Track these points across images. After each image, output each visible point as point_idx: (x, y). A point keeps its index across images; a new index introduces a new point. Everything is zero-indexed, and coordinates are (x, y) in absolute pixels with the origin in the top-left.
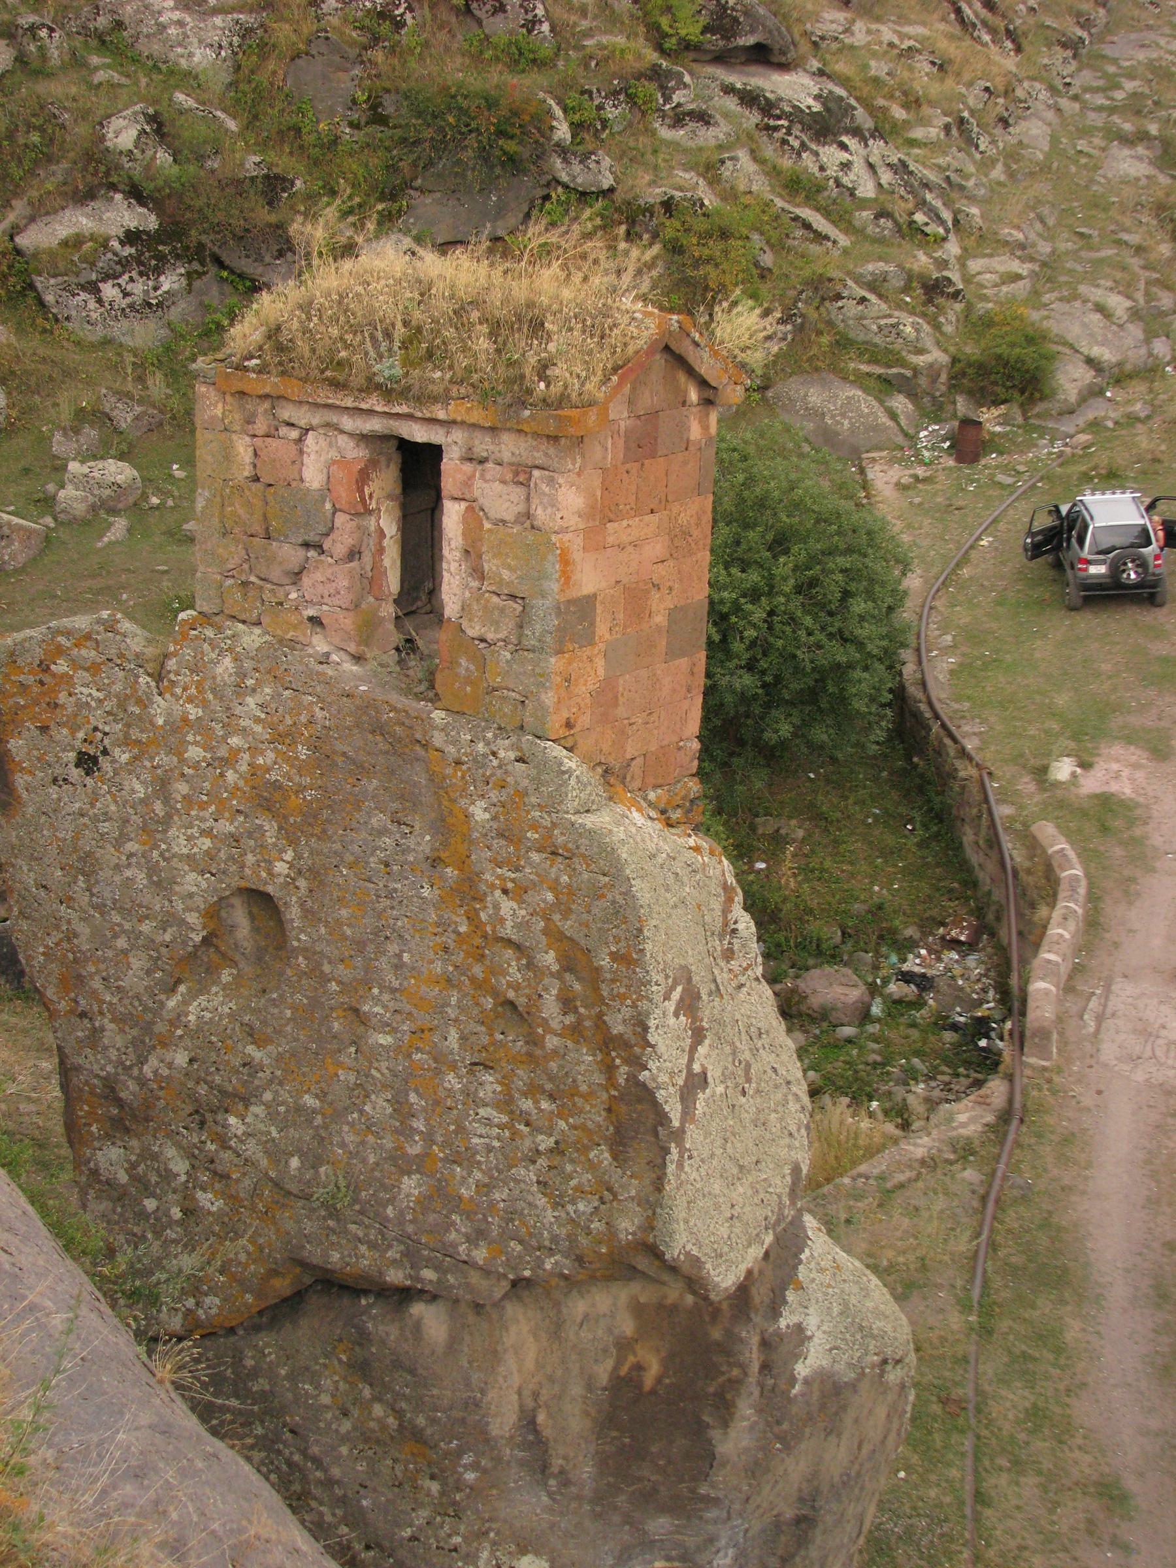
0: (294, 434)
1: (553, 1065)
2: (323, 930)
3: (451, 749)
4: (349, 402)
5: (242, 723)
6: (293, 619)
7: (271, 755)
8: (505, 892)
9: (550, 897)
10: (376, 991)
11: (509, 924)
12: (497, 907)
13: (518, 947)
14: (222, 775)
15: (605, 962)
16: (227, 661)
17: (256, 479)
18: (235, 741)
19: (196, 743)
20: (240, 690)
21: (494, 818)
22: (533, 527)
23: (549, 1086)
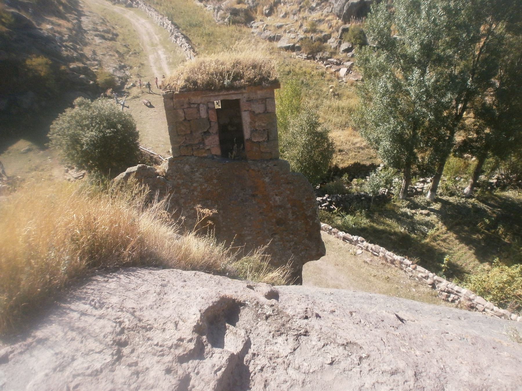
0: (196, 106)
1: (292, 227)
2: (229, 220)
3: (256, 168)
4: (217, 94)
5: (196, 180)
6: (204, 151)
7: (206, 185)
8: (276, 195)
9: (289, 192)
10: (245, 228)
11: (278, 202)
12: (274, 199)
13: (280, 207)
14: (193, 194)
15: (304, 201)
16: (187, 167)
17: (185, 119)
18: (195, 185)
19: (184, 189)
20: (192, 172)
21: (271, 180)
22: (268, 113)
23: (291, 232)
